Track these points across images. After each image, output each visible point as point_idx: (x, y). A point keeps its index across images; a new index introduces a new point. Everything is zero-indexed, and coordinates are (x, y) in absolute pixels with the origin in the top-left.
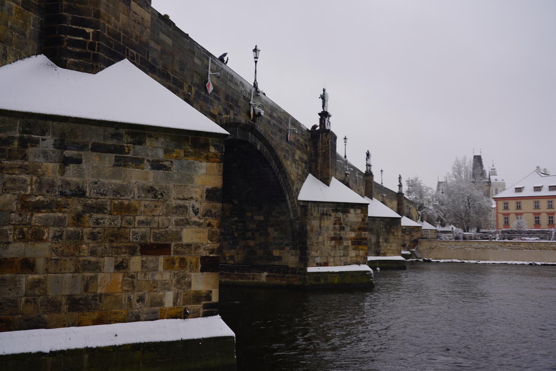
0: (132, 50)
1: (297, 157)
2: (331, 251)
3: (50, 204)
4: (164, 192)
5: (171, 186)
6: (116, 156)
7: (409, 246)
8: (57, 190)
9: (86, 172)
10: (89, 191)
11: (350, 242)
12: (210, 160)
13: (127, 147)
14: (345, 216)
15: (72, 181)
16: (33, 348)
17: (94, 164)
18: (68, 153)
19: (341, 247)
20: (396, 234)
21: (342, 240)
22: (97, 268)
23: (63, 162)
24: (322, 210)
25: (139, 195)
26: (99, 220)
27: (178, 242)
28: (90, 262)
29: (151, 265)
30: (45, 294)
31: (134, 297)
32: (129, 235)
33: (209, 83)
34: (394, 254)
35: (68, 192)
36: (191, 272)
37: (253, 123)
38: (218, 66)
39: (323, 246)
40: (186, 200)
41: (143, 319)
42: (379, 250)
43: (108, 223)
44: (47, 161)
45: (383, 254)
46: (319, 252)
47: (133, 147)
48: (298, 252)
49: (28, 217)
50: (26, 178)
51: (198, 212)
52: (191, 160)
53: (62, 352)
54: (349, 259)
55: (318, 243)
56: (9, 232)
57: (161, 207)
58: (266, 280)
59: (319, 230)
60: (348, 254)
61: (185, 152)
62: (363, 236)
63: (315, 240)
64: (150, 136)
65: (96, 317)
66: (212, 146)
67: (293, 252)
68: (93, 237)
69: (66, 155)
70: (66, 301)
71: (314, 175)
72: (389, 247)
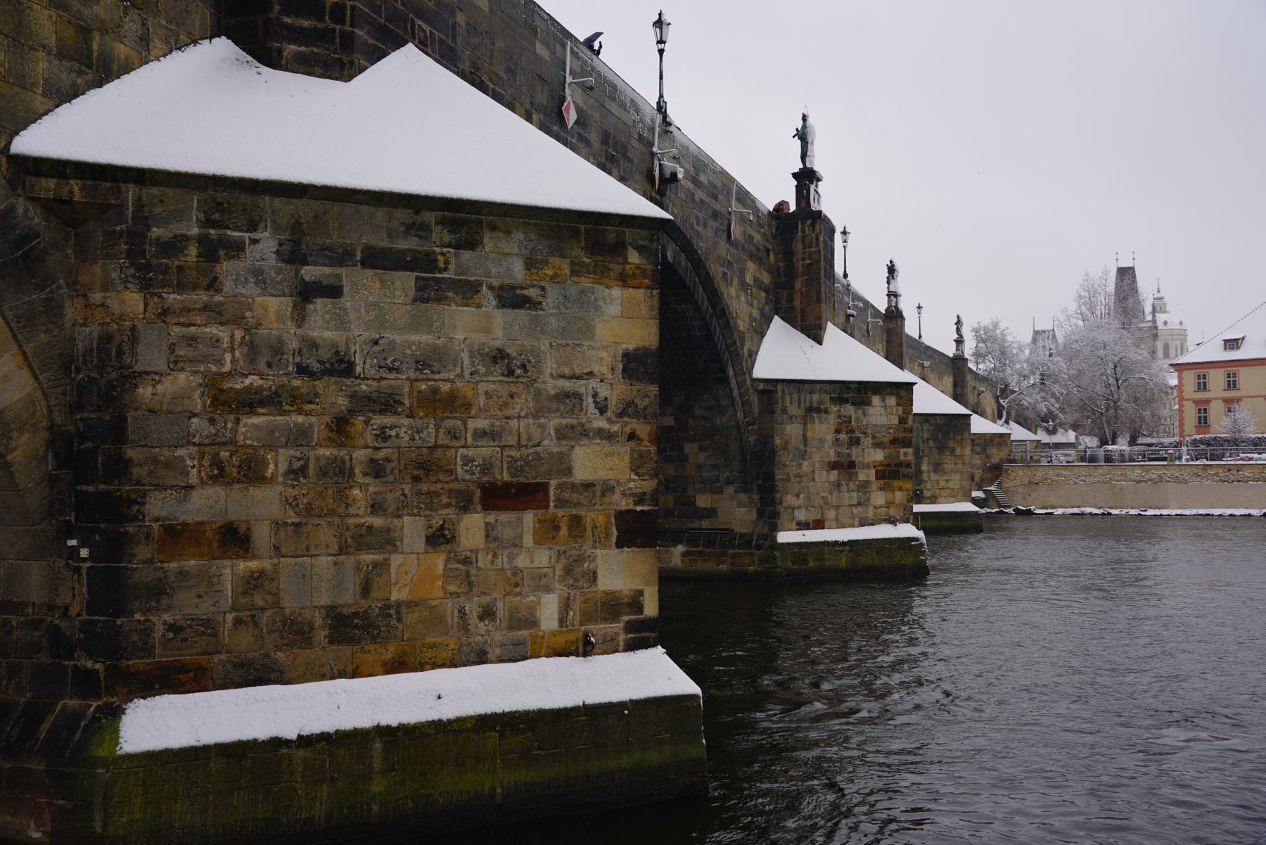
0: (420, 23)
1: (749, 279)
2: (831, 493)
3: (276, 393)
4: (529, 362)
5: (544, 345)
6: (417, 278)
7: (982, 480)
8: (291, 360)
9: (352, 316)
10: (362, 363)
11: (873, 471)
12: (630, 282)
13: (443, 254)
14: (860, 412)
15: (322, 338)
16: (261, 731)
17: (370, 298)
18: (310, 272)
19: (852, 485)
20: (958, 452)
21: (854, 468)
22: (387, 541)
23: (300, 294)
24: (808, 402)
25: (473, 369)
26: (387, 430)
27: (564, 479)
28: (370, 528)
29: (507, 533)
30: (277, 604)
31: (473, 608)
32: (455, 465)
33: (569, 103)
34: (954, 499)
35: (316, 366)
36: (596, 548)
37: (658, 197)
38: (585, 63)
39: (811, 484)
40: (577, 378)
41: (493, 658)
42: (921, 491)
43: (407, 438)
44: (264, 292)
45: (929, 498)
46: (802, 496)
47: (456, 255)
48: (756, 497)
49: (229, 425)
50: (221, 334)
51: (606, 406)
52: (586, 282)
53: (324, 737)
54: (870, 512)
55: (801, 477)
56: (189, 462)
57: (523, 397)
58: (683, 562)
60: (868, 500)
61: (572, 262)
62: (902, 458)
63: (792, 471)
64: (494, 228)
65: (390, 655)
66: (634, 248)
67: (743, 497)
68: (376, 469)
69: (307, 278)
70: (324, 619)
71: (783, 318)
72: (942, 483)
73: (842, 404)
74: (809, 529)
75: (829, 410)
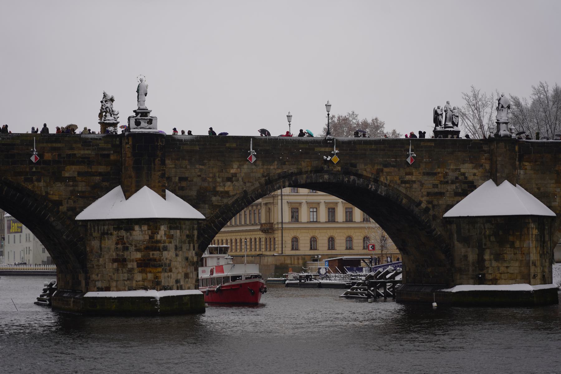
2: (114, 274)
11: (135, 263)
14: (129, 234)
19: (124, 270)
20: (517, 244)
34: (514, 281)
39: (104, 269)
42: (484, 275)
45: (491, 280)
46: (99, 275)
55: (99, 266)
59: (99, 252)
60: (133, 277)
62: (151, 256)
72: (502, 269)
73: (119, 231)
74: (103, 291)
75: (113, 233)
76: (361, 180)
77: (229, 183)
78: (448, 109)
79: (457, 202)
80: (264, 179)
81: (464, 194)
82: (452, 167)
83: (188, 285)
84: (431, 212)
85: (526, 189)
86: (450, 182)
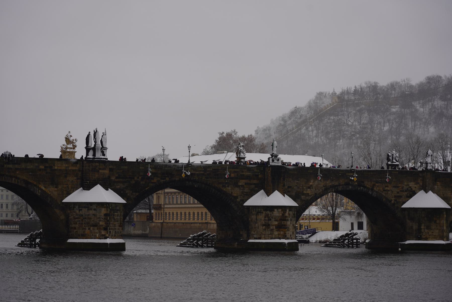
2: (263, 231)
5: (97, 213)
11: (275, 227)
14: (271, 213)
16: (75, 242)
18: (80, 209)
19: (269, 230)
20: (438, 222)
22: (85, 229)
33: (149, 173)
34: (436, 239)
42: (421, 236)
46: (256, 232)
52: (101, 208)
53: (79, 243)
59: (256, 221)
60: (273, 233)
62: (283, 224)
68: (85, 223)
72: (430, 233)
76: (366, 189)
77: (309, 189)
78: (394, 154)
79: (408, 201)
80: (324, 188)
81: (411, 197)
82: (405, 184)
83: (293, 238)
84: (396, 205)
85: (437, 195)
86: (404, 191)
